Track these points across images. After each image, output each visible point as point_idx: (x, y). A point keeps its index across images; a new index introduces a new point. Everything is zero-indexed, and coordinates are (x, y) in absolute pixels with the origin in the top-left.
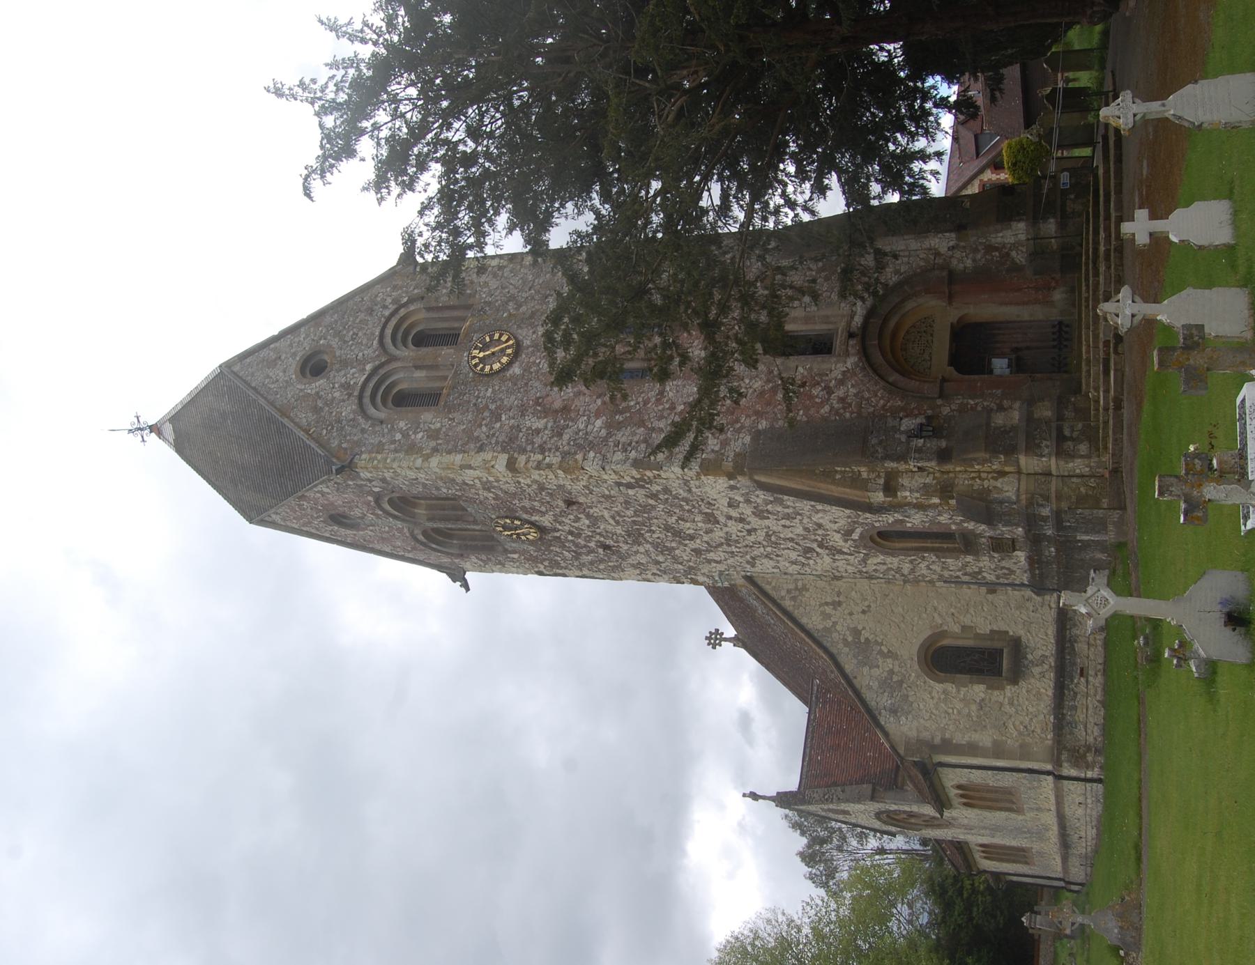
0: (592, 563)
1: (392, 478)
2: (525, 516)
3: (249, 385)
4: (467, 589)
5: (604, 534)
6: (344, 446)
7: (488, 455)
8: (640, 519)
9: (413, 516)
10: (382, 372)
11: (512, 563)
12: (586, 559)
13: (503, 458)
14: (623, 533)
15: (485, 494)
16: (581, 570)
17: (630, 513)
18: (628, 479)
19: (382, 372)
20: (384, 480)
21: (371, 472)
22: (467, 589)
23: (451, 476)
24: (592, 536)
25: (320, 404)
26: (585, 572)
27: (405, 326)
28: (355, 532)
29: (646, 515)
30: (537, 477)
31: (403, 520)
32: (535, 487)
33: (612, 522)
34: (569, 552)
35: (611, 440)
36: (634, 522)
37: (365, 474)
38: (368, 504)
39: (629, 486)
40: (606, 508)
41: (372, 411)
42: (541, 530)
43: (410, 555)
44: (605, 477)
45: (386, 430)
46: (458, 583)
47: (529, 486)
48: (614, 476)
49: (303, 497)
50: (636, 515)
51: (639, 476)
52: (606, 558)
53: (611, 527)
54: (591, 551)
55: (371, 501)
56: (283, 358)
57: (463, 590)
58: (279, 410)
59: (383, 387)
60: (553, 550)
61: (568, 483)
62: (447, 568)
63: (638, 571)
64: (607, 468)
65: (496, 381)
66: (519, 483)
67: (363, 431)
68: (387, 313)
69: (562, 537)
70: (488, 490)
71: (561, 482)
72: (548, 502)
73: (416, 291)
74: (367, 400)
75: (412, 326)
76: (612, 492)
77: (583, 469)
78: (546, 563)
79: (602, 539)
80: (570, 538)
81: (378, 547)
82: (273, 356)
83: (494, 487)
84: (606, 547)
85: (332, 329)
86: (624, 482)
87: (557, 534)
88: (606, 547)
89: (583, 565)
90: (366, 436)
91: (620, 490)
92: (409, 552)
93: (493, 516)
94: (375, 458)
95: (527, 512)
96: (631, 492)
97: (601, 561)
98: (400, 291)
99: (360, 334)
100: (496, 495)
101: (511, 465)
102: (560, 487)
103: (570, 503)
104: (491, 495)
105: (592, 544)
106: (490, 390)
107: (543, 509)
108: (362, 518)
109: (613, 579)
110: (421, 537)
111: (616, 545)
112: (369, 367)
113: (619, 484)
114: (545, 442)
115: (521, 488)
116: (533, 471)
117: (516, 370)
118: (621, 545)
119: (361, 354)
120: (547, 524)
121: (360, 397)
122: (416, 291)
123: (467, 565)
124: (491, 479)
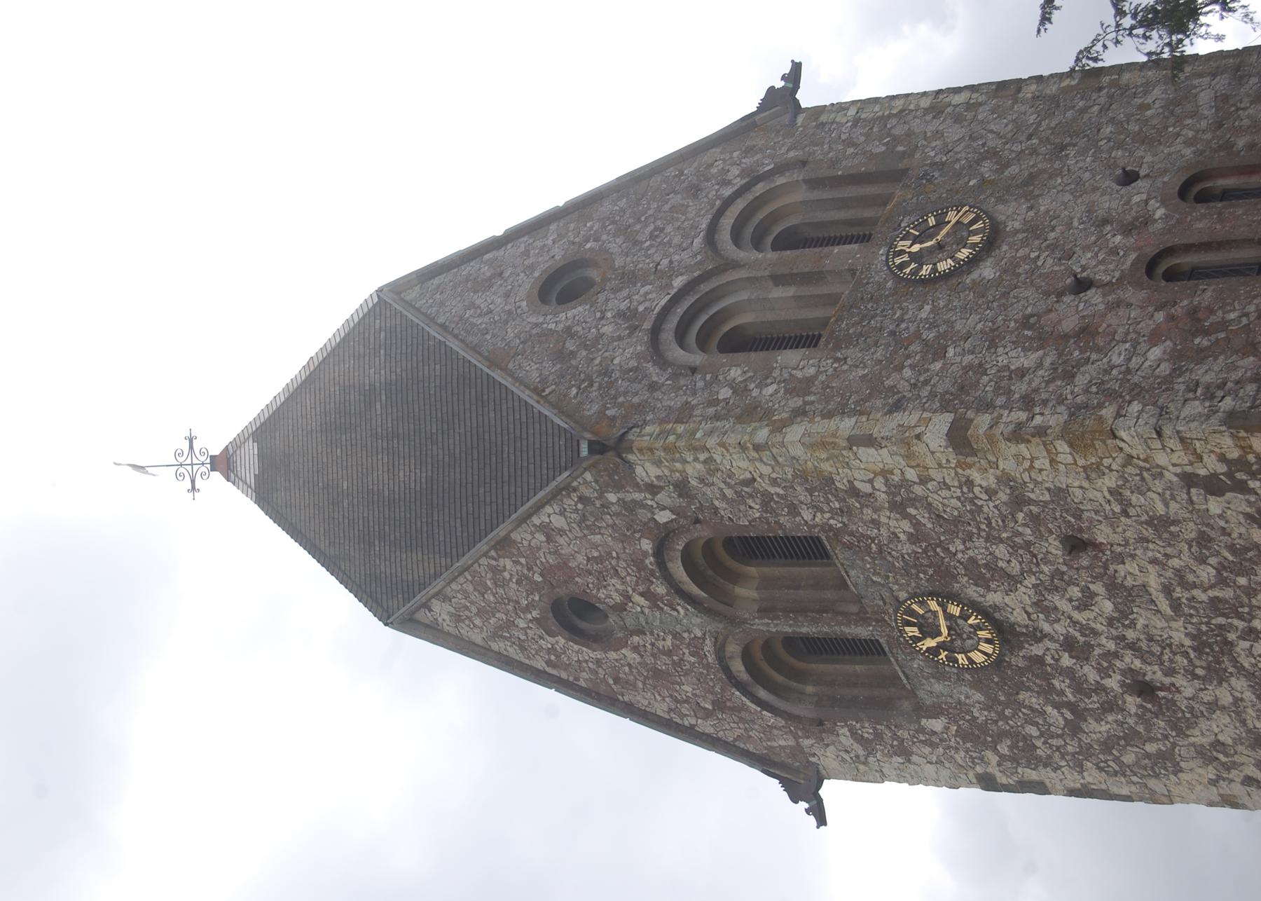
0: (1107, 745)
1: (702, 480)
2: (973, 592)
3: (432, 320)
4: (822, 821)
5: (1144, 645)
6: (609, 413)
7: (909, 418)
8: (1227, 594)
9: (729, 600)
10: (705, 288)
11: (927, 750)
12: (1097, 729)
13: (943, 422)
14: (1187, 642)
15: (893, 523)
16: (1081, 769)
17: (1206, 573)
18: (1212, 465)
19: (705, 288)
20: (682, 487)
21: (658, 463)
22: (822, 821)
23: (827, 467)
24: (1116, 655)
25: (570, 345)
26: (1092, 776)
27: (761, 215)
28: (598, 655)
29: (1242, 581)
30: (1007, 465)
31: (708, 612)
32: (1003, 496)
33: (1164, 605)
34: (1057, 706)
35: (1180, 380)
36: (1214, 601)
37: (646, 471)
38: (638, 563)
39: (1213, 486)
40: (1154, 561)
41: (676, 353)
42: (1005, 634)
43: (706, 726)
44: (1161, 459)
45: (700, 384)
46: (803, 805)
47: (991, 493)
48: (1181, 457)
49: (504, 545)
50: (1222, 582)
51: (1235, 454)
52: (1141, 728)
53: (1160, 624)
54: (1111, 706)
55: (645, 554)
56: (506, 274)
57: (812, 820)
58: (487, 359)
59: (704, 318)
60: (1021, 705)
61: (1075, 482)
62: (784, 766)
63: (1210, 773)
64: (1167, 431)
65: (941, 296)
66: (970, 483)
67: (653, 387)
68: (727, 192)
69: (1049, 660)
70: (899, 508)
71: (1062, 481)
72: (1028, 544)
73: (791, 154)
74: (668, 335)
75: (774, 218)
76: (1173, 505)
77: (1115, 437)
78: (1004, 748)
79: (1137, 664)
80: (1067, 661)
81: (641, 700)
82: (487, 271)
83: (913, 501)
84: (1145, 689)
85: (614, 222)
86: (1202, 472)
87: (1037, 650)
88: (1145, 689)
89: (1087, 752)
90: (658, 394)
91: (1191, 501)
92: (708, 715)
93: (903, 595)
94: (672, 432)
95: (980, 581)
96: (1215, 506)
97: (1131, 737)
98: (759, 156)
99: (669, 229)
100: (917, 524)
101: (959, 439)
102: (1060, 494)
103: (1076, 545)
104: (906, 525)
105: (1113, 683)
106: (927, 308)
107: (1015, 568)
108: (621, 608)
109: (1153, 799)
110: (738, 667)
111: (1167, 680)
112: (678, 282)
113: (1189, 480)
114: (1036, 390)
115: (972, 501)
116: (1003, 445)
117: (987, 271)
118: (1180, 681)
119: (665, 262)
120: (1018, 617)
121: (656, 331)
122: (791, 154)
123: (827, 757)
124: (911, 475)
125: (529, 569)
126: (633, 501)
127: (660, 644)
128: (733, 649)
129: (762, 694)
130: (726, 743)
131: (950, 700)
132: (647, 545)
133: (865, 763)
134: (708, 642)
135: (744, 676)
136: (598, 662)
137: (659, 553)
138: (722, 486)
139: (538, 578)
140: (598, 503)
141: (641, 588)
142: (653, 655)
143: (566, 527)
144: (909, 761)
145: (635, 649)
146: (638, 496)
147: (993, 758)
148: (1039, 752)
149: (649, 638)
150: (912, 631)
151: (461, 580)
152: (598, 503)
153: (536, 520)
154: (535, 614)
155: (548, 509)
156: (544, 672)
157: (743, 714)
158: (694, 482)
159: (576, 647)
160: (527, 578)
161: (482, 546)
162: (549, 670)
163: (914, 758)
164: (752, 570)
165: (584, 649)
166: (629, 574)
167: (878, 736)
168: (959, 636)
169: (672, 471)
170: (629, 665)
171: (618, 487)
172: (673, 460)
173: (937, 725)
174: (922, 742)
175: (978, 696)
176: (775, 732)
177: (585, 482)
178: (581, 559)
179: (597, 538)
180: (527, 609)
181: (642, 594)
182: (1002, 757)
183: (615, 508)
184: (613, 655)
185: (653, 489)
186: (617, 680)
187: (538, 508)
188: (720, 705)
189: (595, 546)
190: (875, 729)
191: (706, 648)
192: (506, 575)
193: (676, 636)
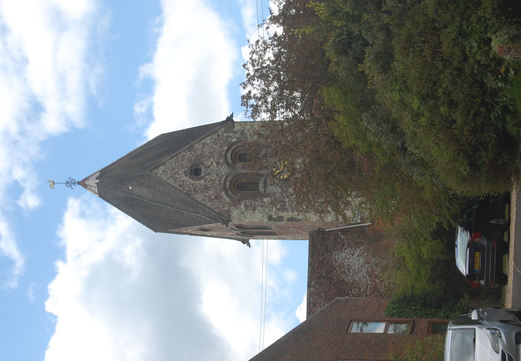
1: (248, 130)
38: (220, 154)
55: (224, 150)
78: (278, 207)
92: (212, 200)
110: (228, 184)
125: (193, 156)
126: (230, 136)
127: (212, 178)
128: (230, 178)
129: (229, 192)
130: (212, 209)
131: (273, 191)
132: (226, 148)
133: (243, 214)
134: (224, 177)
135: (228, 187)
136: (193, 184)
137: (228, 149)
138: (252, 132)
139: (193, 158)
140: (221, 136)
141: (217, 161)
142: (208, 182)
143: (209, 143)
144: (254, 212)
145: (205, 180)
146: (231, 134)
147: (274, 209)
148: (286, 207)
149: (210, 176)
150: (274, 169)
151: (173, 159)
152: (221, 136)
153: (203, 141)
154: (186, 169)
155: (208, 138)
156: (177, 188)
157: (221, 200)
158: (246, 131)
159: (190, 179)
160: (190, 158)
161: (187, 147)
162: (179, 188)
163: (256, 211)
164: (242, 163)
165: (192, 180)
166: (217, 157)
167: (251, 204)
168: (283, 172)
169: (243, 128)
170: (200, 185)
171: (228, 132)
172: (245, 125)
173: (265, 200)
174: (260, 206)
175: (280, 190)
176: (226, 205)
177: (221, 131)
178: (208, 152)
179: (214, 146)
180: (184, 168)
181: (216, 163)
182: (277, 209)
183: (224, 138)
184: (198, 182)
185: (236, 132)
186: (194, 190)
187: (204, 138)
188: (216, 197)
189: (213, 148)
190: (251, 202)
191: (223, 178)
192: (186, 157)
193: (217, 175)
